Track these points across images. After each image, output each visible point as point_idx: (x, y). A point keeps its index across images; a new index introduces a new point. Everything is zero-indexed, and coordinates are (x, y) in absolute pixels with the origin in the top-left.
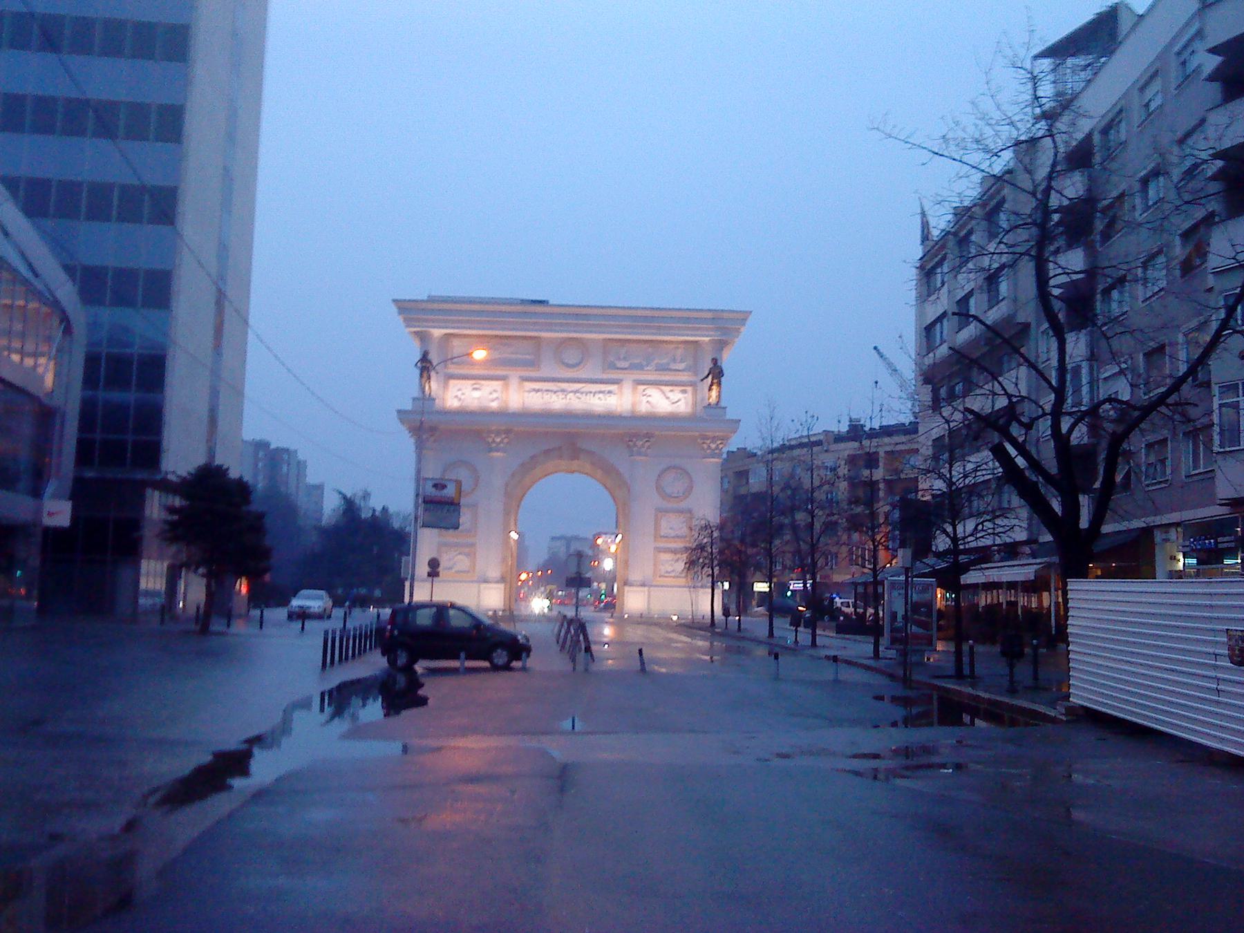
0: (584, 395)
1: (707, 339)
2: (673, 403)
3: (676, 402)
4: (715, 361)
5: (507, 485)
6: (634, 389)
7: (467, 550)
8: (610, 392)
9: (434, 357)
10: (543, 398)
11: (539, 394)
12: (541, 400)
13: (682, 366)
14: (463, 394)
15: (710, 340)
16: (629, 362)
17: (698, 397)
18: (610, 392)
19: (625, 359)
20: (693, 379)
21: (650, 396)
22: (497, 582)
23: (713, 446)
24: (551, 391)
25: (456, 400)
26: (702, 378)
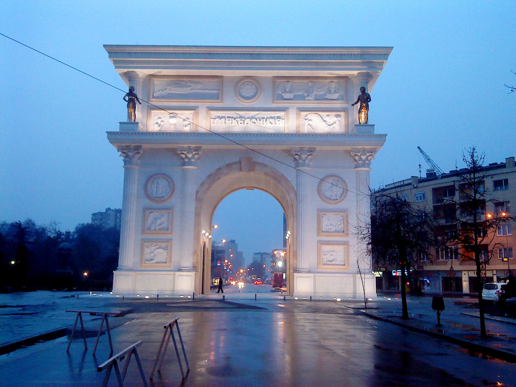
0: (258, 120)
1: (355, 73)
2: (330, 125)
3: (332, 124)
4: (363, 90)
5: (197, 192)
6: (298, 115)
7: (164, 245)
8: (279, 118)
9: (139, 92)
10: (225, 123)
11: (223, 120)
12: (224, 125)
13: (336, 96)
14: (162, 121)
15: (359, 73)
16: (293, 94)
17: (350, 120)
18: (279, 118)
19: (290, 92)
20: (345, 105)
21: (310, 120)
22: (188, 271)
23: (363, 157)
24: (233, 118)
25: (156, 125)
26: (353, 103)
